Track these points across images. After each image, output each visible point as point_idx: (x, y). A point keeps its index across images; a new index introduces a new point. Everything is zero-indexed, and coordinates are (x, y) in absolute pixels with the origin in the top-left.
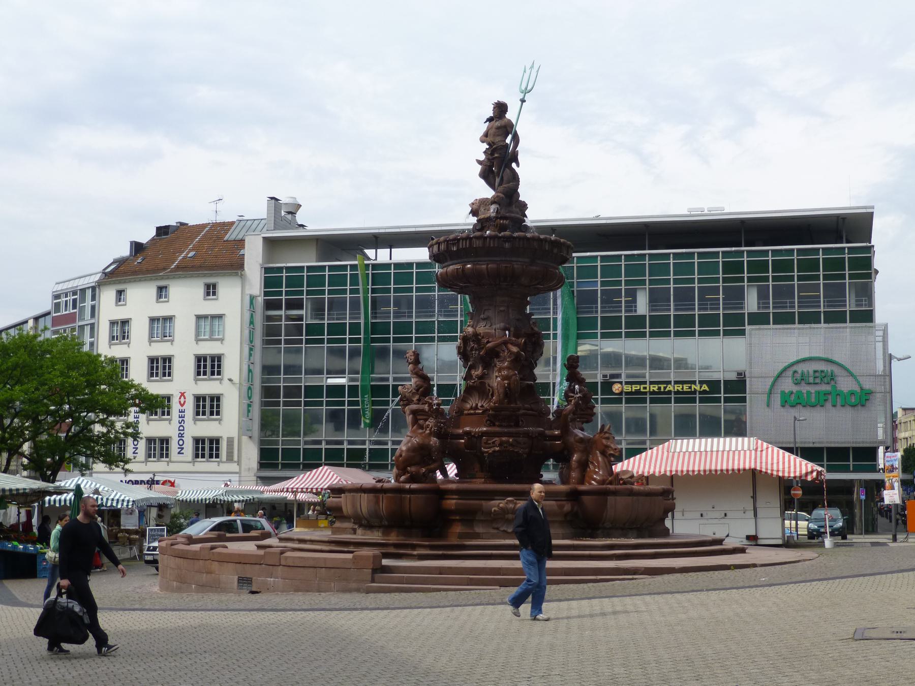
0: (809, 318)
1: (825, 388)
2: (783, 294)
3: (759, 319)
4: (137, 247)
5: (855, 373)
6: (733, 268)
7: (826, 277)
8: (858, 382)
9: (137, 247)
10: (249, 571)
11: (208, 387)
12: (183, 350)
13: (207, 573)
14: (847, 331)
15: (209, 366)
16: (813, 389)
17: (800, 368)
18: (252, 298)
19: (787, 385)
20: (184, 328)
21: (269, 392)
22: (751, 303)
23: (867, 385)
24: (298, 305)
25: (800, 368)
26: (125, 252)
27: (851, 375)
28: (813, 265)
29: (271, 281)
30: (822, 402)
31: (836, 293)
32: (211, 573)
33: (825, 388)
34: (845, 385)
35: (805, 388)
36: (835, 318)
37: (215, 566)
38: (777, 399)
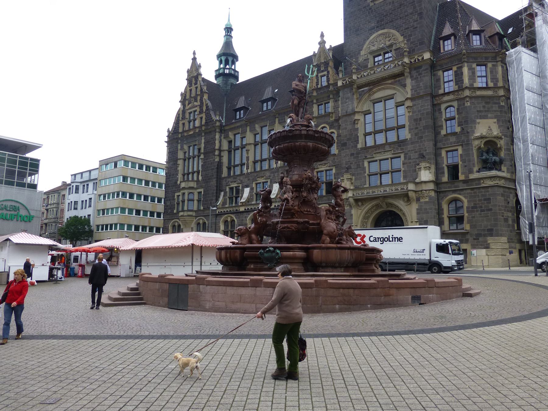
0: (11, 184)
5: (28, 208)
7: (19, 168)
8: (29, 212)
10: (418, 292)
13: (385, 296)
14: (27, 191)
16: (9, 213)
17: (4, 203)
23: (32, 213)
25: (4, 203)
27: (27, 209)
28: (15, 162)
30: (13, 218)
31: (22, 175)
32: (389, 295)
34: (23, 212)
35: (5, 212)
37: (393, 291)
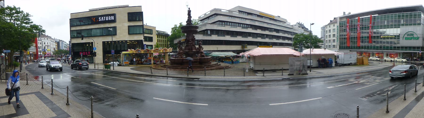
1: (412, 36)
2: (407, 21)
3: (403, 25)
4: (331, 21)
6: (399, 16)
9: (331, 21)
11: (334, 38)
12: (332, 34)
15: (334, 35)
18: (337, 26)
19: (406, 36)
20: (332, 31)
21: (340, 39)
22: (402, 22)
24: (342, 27)
26: (329, 22)
29: (340, 24)
33: (412, 36)
34: (415, 36)
36: (415, 24)
38: (404, 38)
